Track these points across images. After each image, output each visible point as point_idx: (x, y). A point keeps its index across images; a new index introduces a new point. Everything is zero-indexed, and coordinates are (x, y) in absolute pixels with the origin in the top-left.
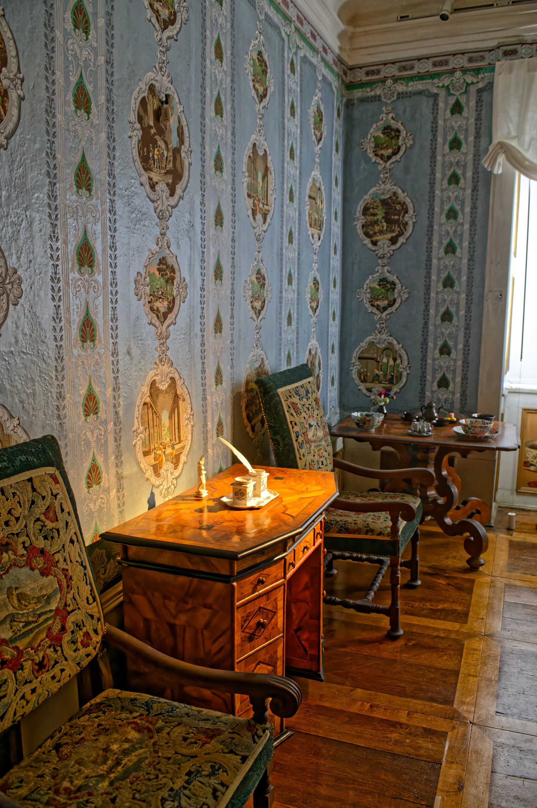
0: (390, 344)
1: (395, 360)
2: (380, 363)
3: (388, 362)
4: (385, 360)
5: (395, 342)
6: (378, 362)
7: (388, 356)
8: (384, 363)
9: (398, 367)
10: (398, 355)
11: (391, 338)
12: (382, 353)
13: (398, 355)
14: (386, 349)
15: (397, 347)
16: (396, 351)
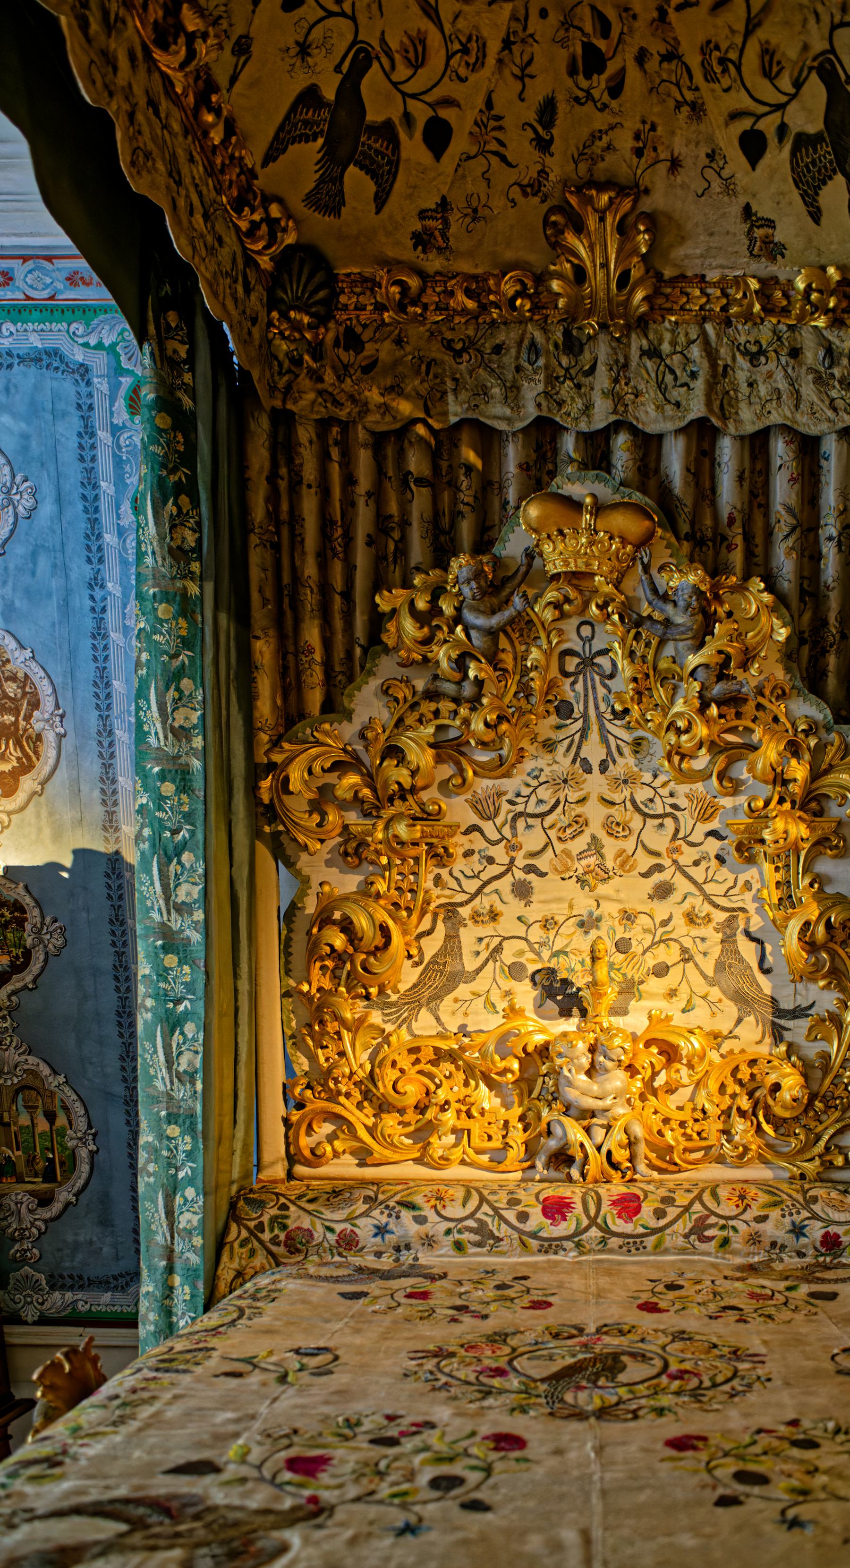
0: (34, 1073)
1: (51, 1117)
2: (14, 1128)
3: (34, 1125)
4: (24, 1119)
5: (45, 1070)
6: (8, 1125)
7: (31, 1109)
8: (21, 1127)
9: (62, 1133)
10: (58, 1103)
11: (32, 1059)
12: (14, 1100)
13: (58, 1103)
14: (22, 1088)
15: (54, 1082)
16: (52, 1094)
